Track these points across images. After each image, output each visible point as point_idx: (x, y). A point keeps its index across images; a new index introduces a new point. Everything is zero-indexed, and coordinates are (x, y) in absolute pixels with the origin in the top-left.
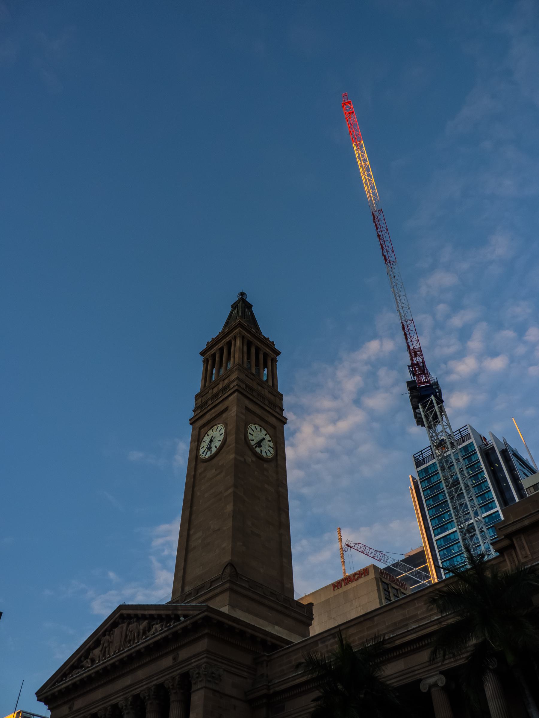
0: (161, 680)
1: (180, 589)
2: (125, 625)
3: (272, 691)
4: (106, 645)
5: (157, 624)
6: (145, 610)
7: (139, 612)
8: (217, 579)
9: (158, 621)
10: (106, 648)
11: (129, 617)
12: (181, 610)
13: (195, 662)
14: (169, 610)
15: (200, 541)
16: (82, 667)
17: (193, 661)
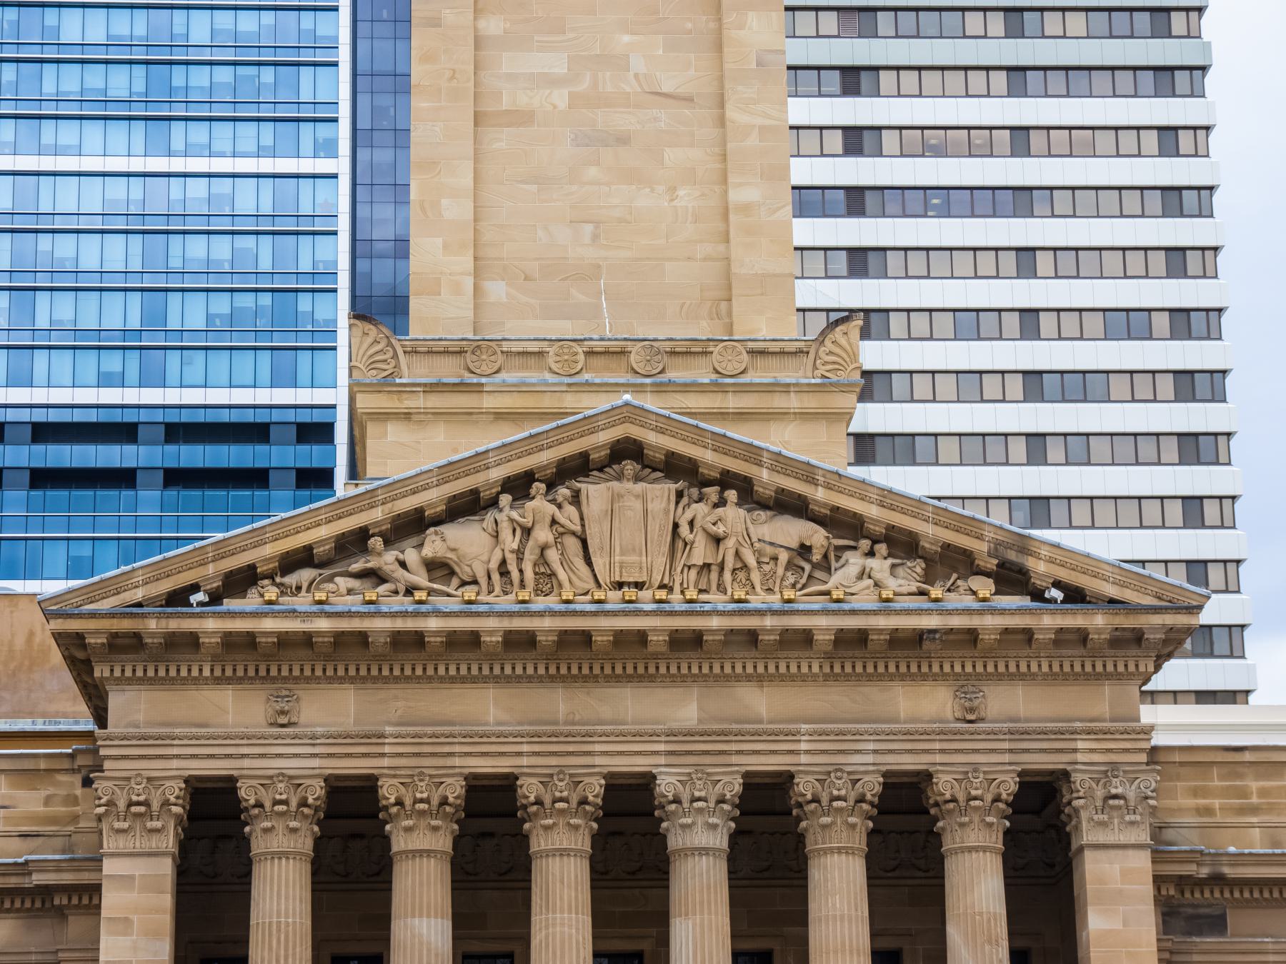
0: (909, 763)
1: (469, 282)
2: (661, 492)
3: (1204, 872)
4: (543, 534)
5: (871, 554)
6: (814, 482)
7: (765, 475)
8: (782, 353)
9: (882, 548)
10: (543, 549)
11: (677, 468)
12: (1051, 561)
13: (1092, 751)
14: (980, 537)
15: (560, 98)
16: (375, 576)
17: (1080, 745)
